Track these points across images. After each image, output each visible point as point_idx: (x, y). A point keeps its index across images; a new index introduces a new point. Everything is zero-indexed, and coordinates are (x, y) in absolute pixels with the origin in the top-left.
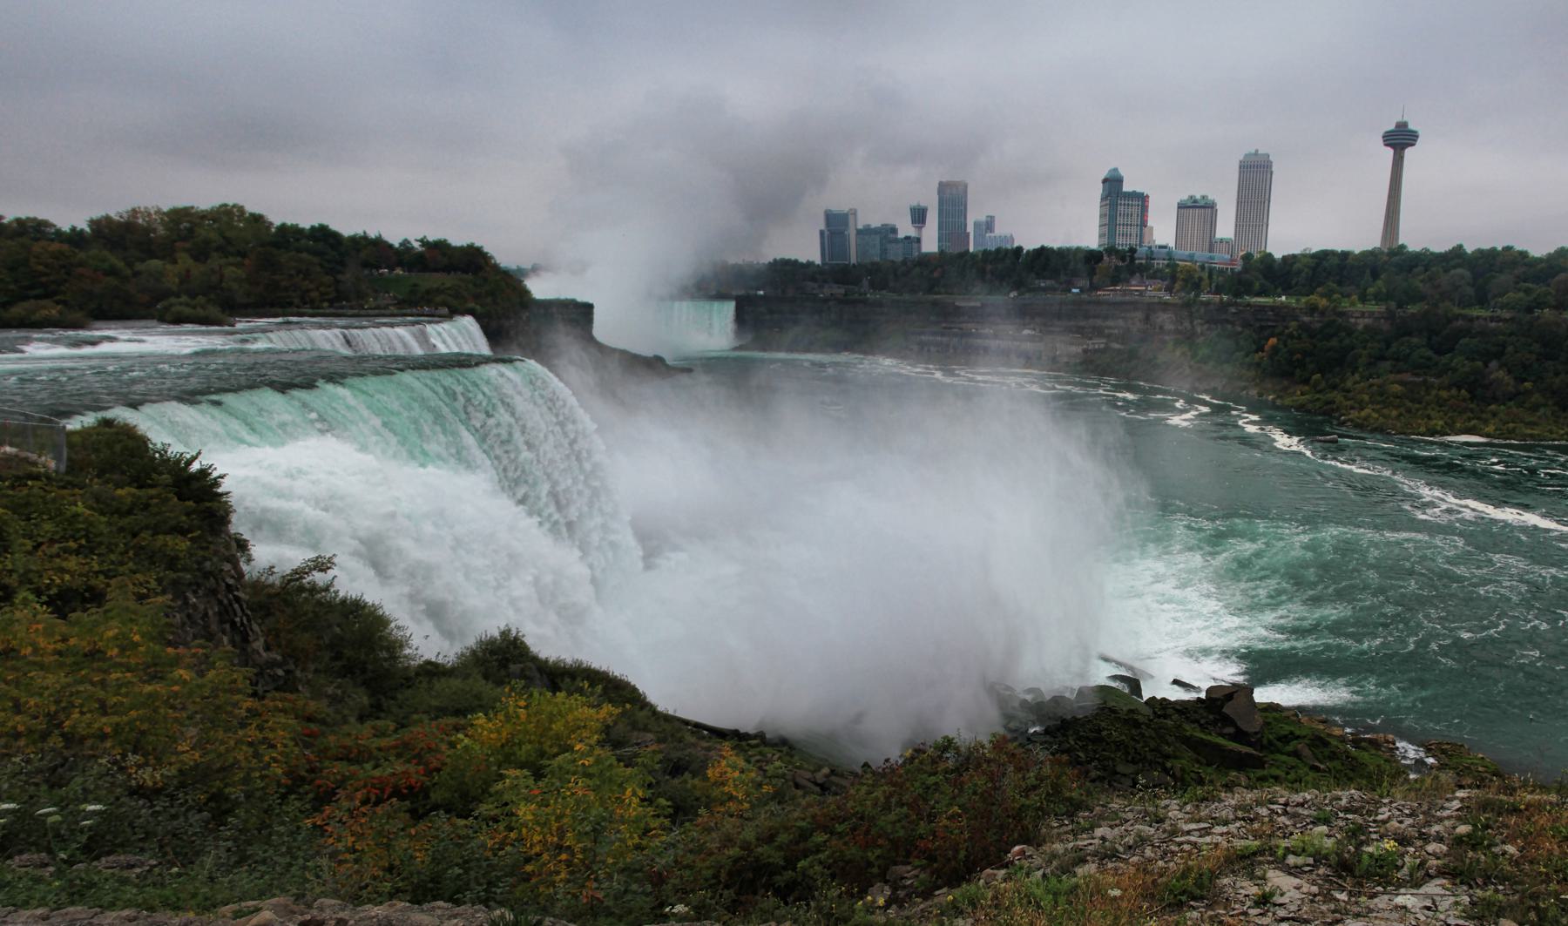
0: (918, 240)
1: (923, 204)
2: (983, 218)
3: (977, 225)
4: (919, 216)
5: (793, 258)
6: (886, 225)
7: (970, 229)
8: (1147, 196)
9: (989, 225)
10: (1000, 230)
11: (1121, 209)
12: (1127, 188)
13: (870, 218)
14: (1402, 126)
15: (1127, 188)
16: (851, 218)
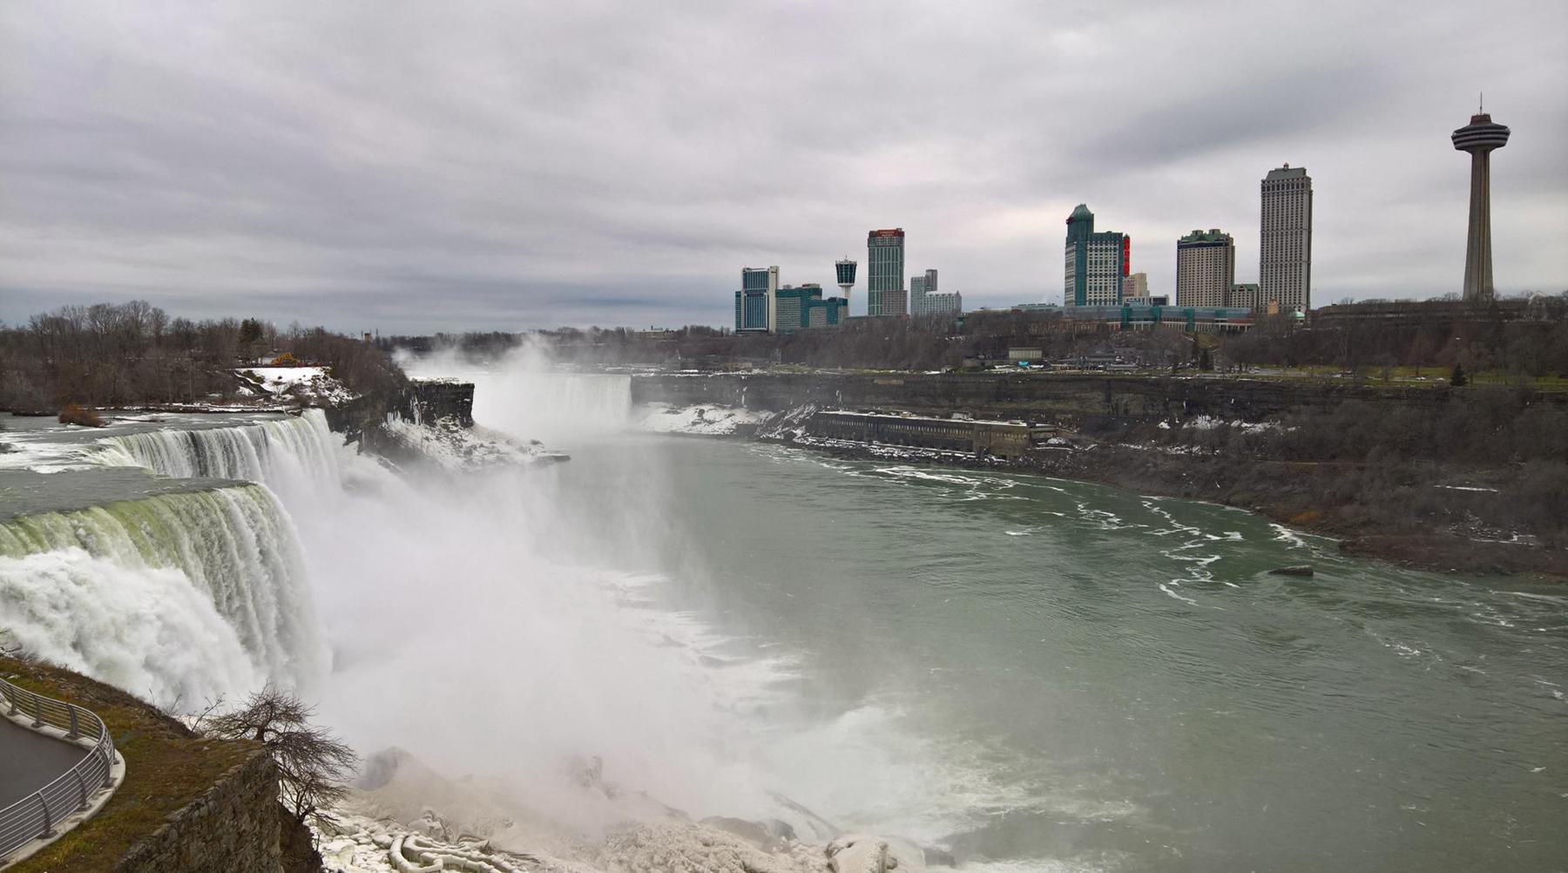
0: (845, 302)
1: (851, 259)
2: (923, 274)
3: (914, 281)
4: (846, 272)
5: (705, 325)
6: (808, 285)
7: (907, 286)
8: (1127, 239)
9: (930, 280)
10: (944, 287)
11: (1092, 256)
12: (1100, 227)
13: (793, 275)
14: (1481, 121)
15: (1100, 227)
16: (771, 277)
